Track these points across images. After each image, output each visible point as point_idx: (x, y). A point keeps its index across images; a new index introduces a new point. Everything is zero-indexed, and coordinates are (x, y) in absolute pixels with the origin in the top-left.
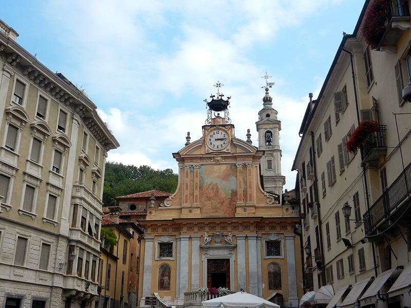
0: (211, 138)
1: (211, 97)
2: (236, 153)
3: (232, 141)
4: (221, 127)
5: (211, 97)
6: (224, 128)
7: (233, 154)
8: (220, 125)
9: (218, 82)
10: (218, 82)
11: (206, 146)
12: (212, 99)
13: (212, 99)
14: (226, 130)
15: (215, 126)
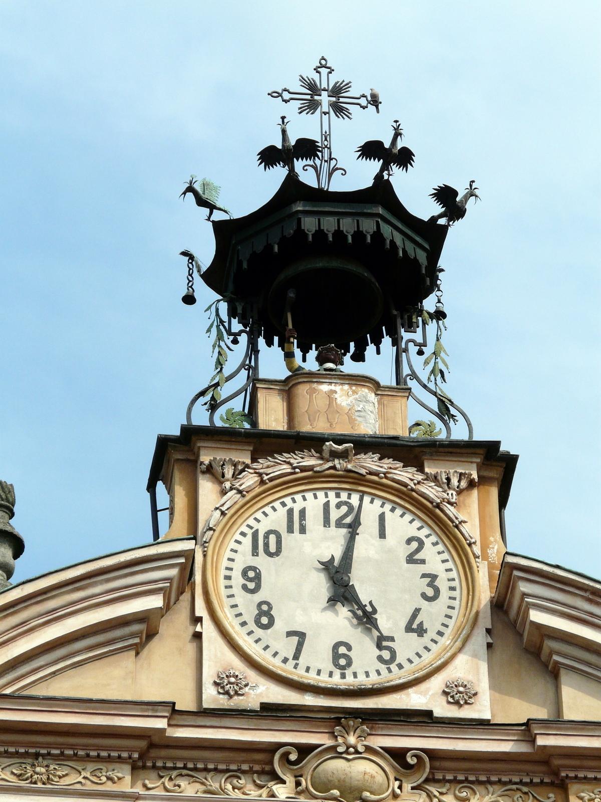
0: (262, 562)
1: (269, 157)
2: (557, 723)
3: (499, 605)
4: (369, 462)
5: (269, 157)
6: (405, 475)
7: (527, 729)
8: (363, 445)
9: (323, 65)
10: (323, 65)
11: (207, 628)
12: (279, 173)
13: (279, 173)
14: (431, 491)
15: (313, 442)
